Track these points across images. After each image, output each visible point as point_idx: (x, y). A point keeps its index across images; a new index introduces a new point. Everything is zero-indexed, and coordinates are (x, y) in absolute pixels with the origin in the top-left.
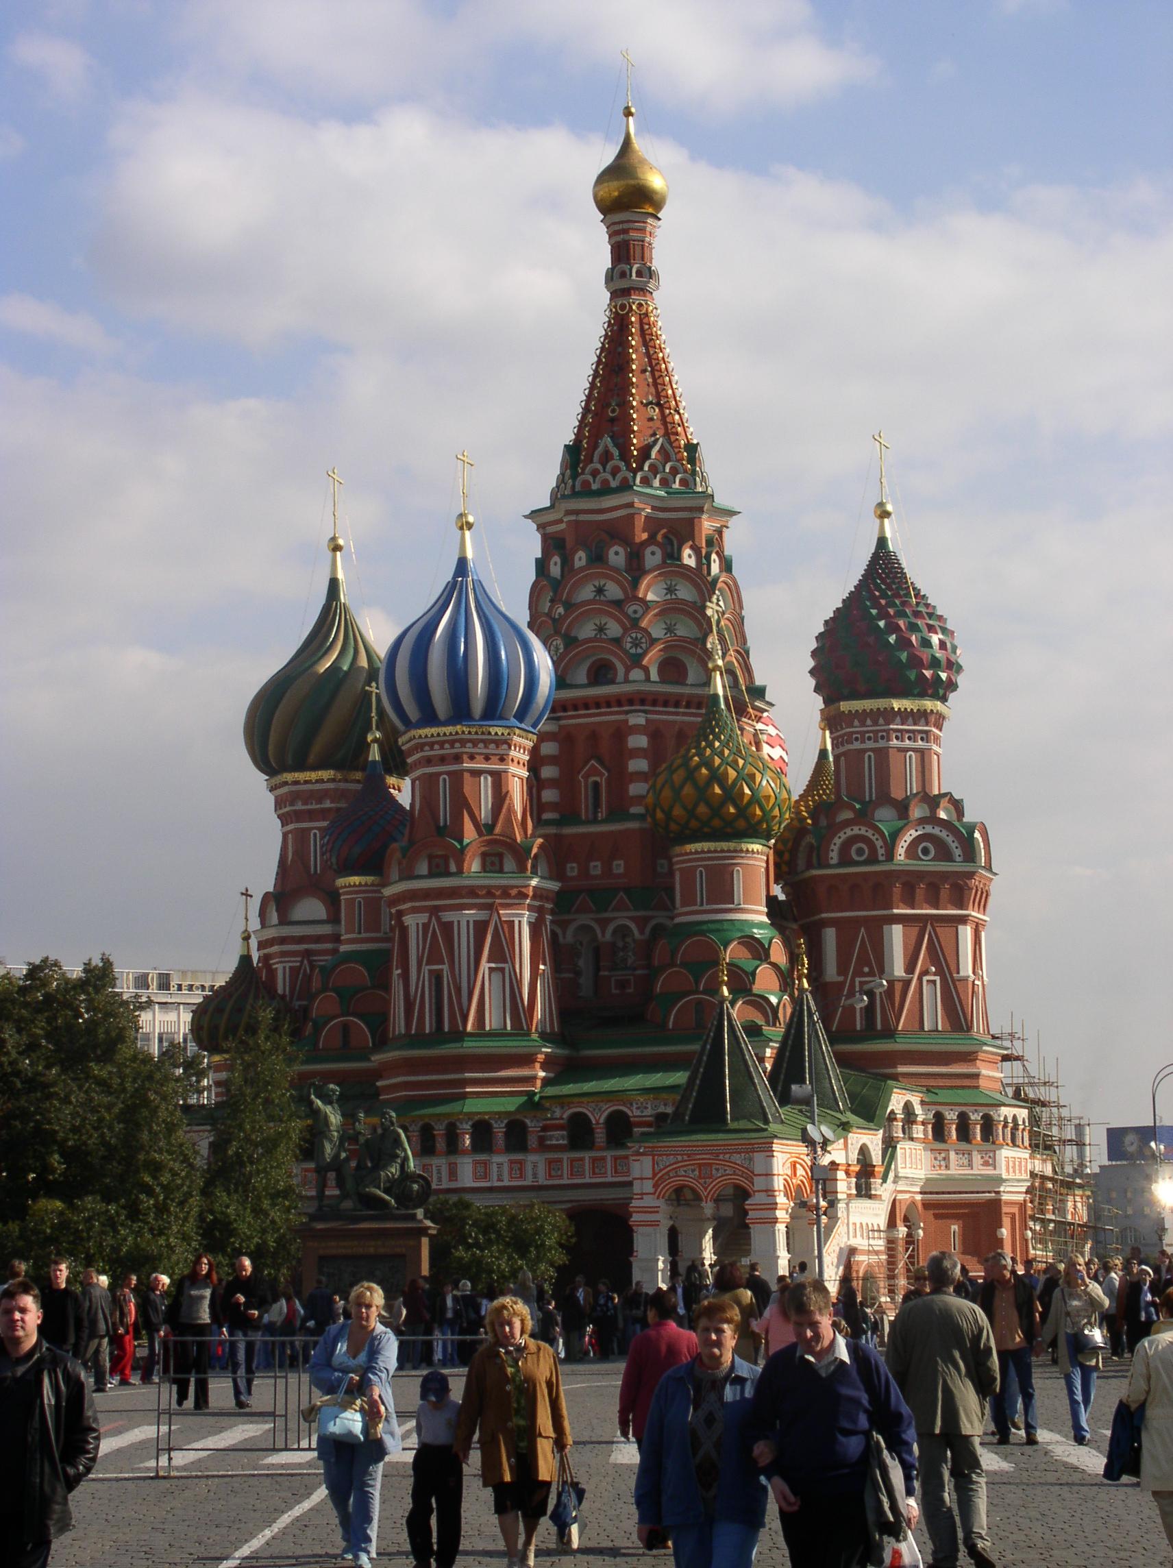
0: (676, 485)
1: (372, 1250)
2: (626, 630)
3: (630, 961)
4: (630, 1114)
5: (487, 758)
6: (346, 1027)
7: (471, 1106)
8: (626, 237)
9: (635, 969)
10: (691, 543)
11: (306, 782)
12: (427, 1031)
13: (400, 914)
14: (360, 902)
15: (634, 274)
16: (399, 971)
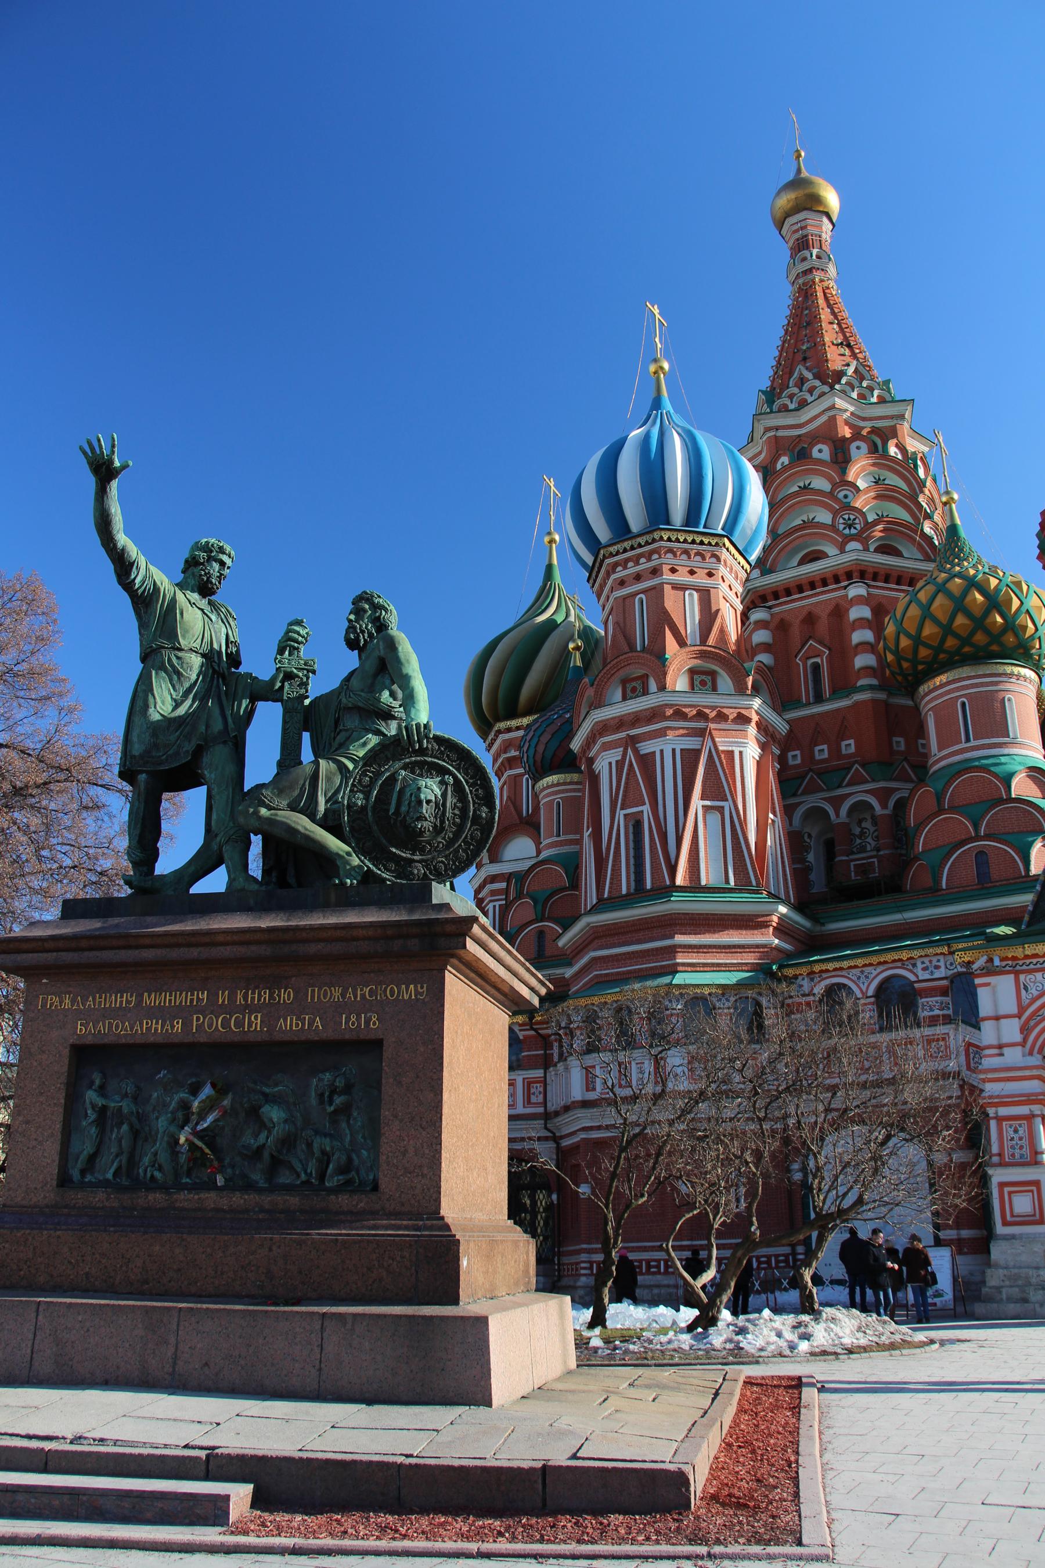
0: (874, 400)
1: (256, 1022)
2: (835, 513)
3: (869, 848)
4: (913, 978)
5: (692, 573)
6: (541, 933)
7: (679, 979)
8: (805, 232)
9: (878, 850)
10: (895, 441)
11: (518, 728)
12: (624, 891)
13: (591, 761)
14: (559, 803)
15: (814, 257)
16: (590, 830)
